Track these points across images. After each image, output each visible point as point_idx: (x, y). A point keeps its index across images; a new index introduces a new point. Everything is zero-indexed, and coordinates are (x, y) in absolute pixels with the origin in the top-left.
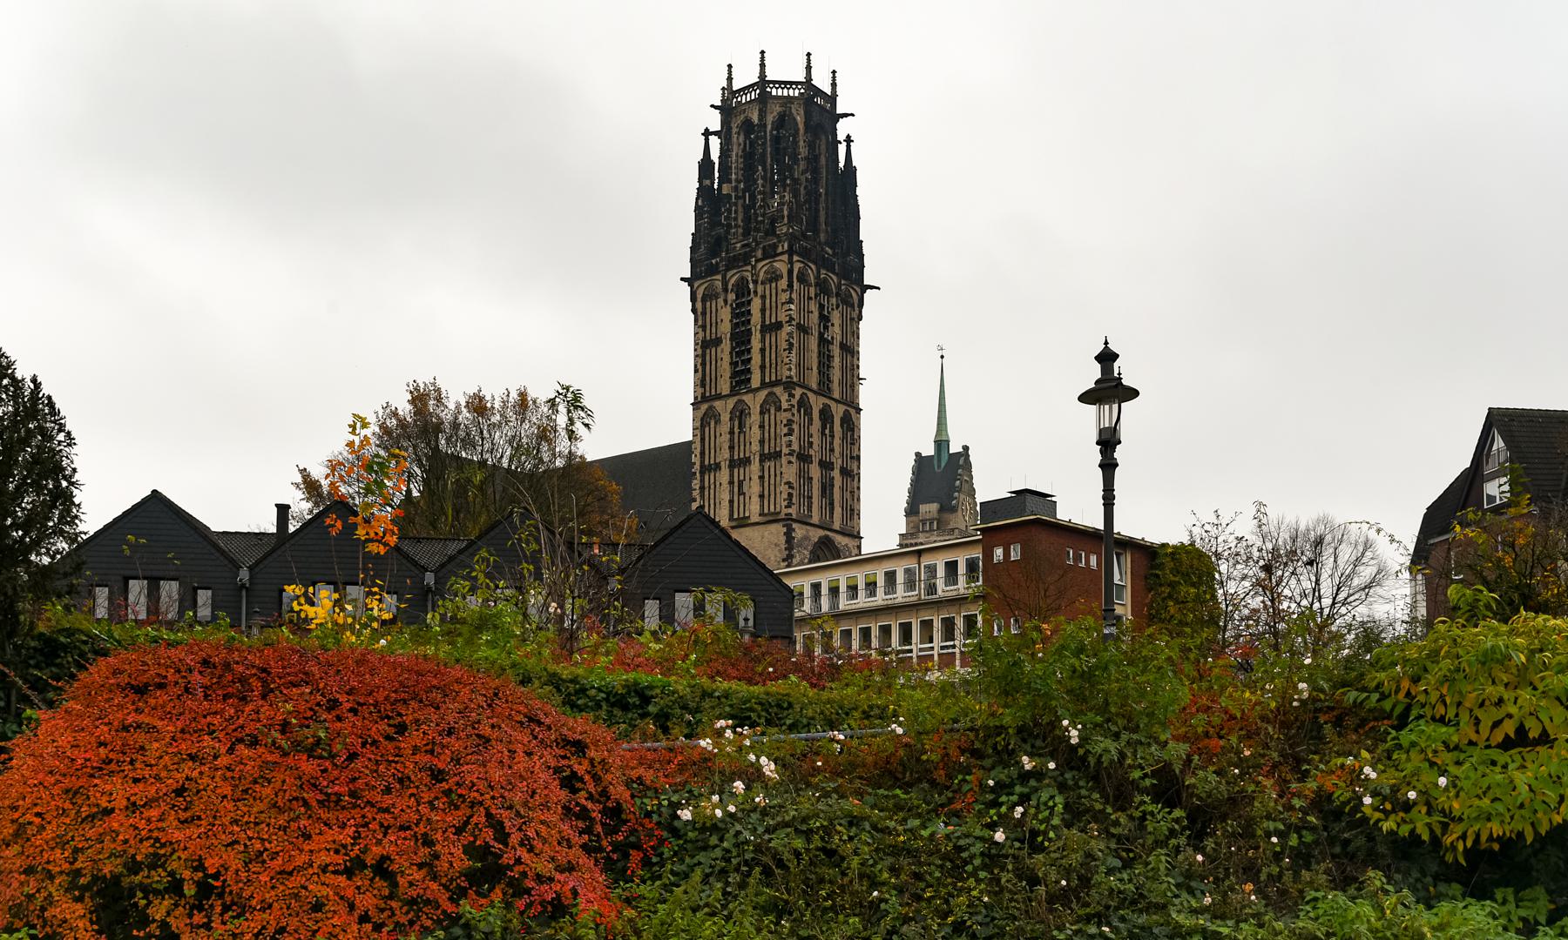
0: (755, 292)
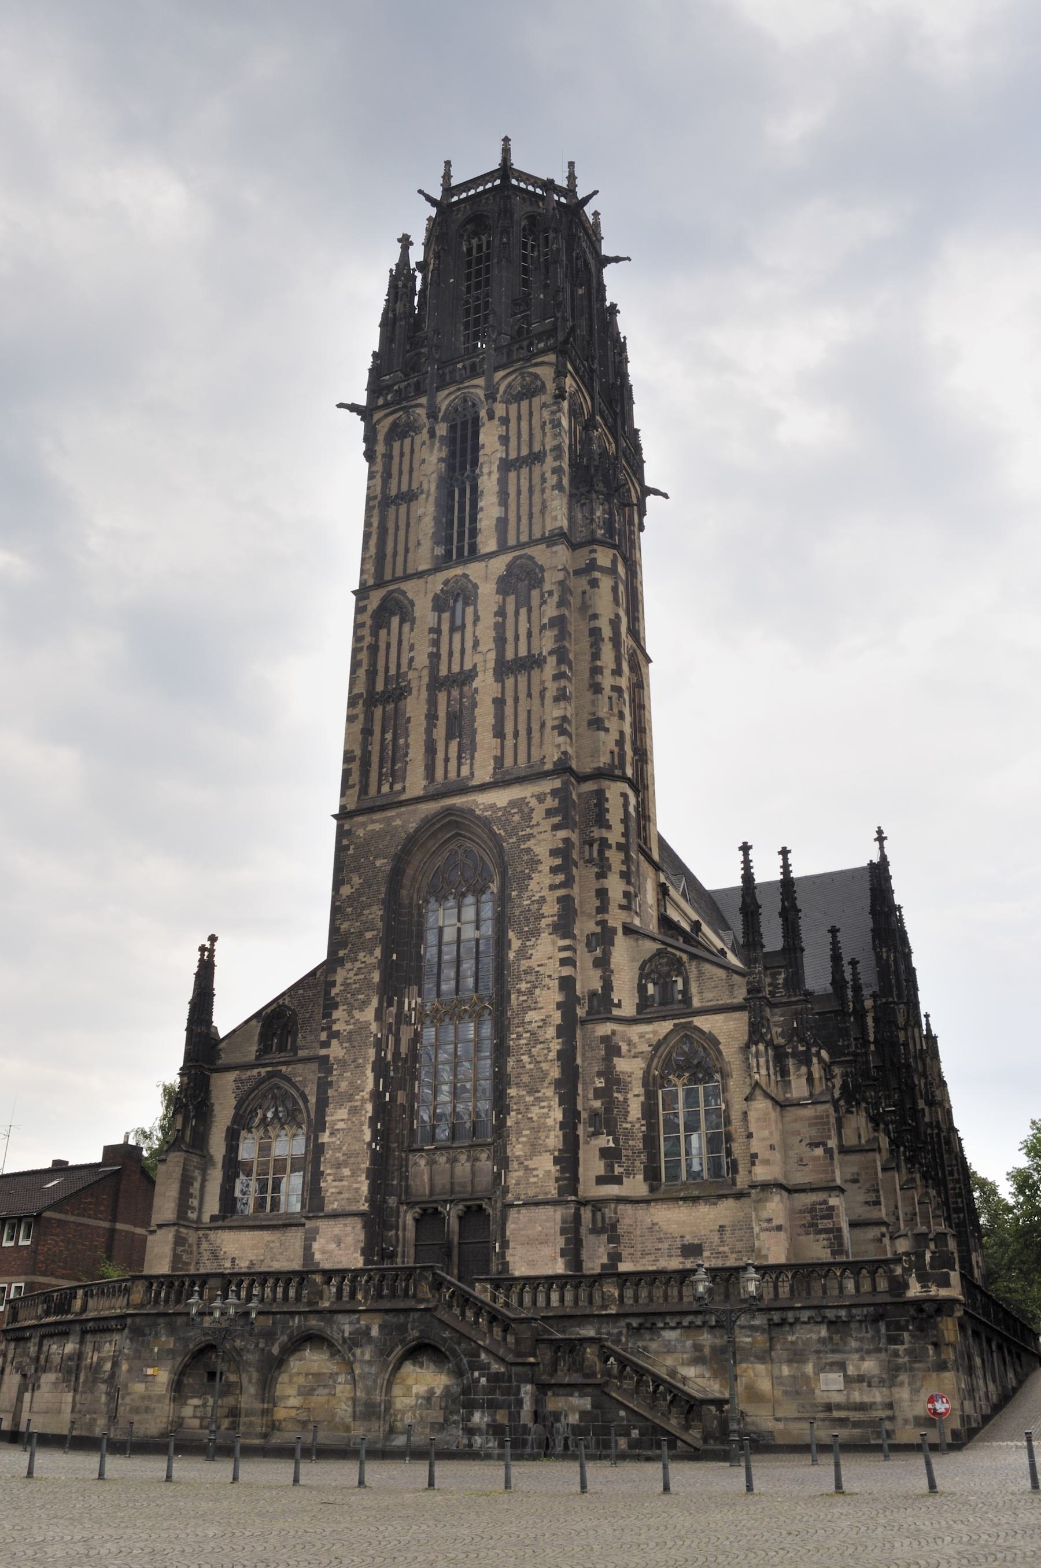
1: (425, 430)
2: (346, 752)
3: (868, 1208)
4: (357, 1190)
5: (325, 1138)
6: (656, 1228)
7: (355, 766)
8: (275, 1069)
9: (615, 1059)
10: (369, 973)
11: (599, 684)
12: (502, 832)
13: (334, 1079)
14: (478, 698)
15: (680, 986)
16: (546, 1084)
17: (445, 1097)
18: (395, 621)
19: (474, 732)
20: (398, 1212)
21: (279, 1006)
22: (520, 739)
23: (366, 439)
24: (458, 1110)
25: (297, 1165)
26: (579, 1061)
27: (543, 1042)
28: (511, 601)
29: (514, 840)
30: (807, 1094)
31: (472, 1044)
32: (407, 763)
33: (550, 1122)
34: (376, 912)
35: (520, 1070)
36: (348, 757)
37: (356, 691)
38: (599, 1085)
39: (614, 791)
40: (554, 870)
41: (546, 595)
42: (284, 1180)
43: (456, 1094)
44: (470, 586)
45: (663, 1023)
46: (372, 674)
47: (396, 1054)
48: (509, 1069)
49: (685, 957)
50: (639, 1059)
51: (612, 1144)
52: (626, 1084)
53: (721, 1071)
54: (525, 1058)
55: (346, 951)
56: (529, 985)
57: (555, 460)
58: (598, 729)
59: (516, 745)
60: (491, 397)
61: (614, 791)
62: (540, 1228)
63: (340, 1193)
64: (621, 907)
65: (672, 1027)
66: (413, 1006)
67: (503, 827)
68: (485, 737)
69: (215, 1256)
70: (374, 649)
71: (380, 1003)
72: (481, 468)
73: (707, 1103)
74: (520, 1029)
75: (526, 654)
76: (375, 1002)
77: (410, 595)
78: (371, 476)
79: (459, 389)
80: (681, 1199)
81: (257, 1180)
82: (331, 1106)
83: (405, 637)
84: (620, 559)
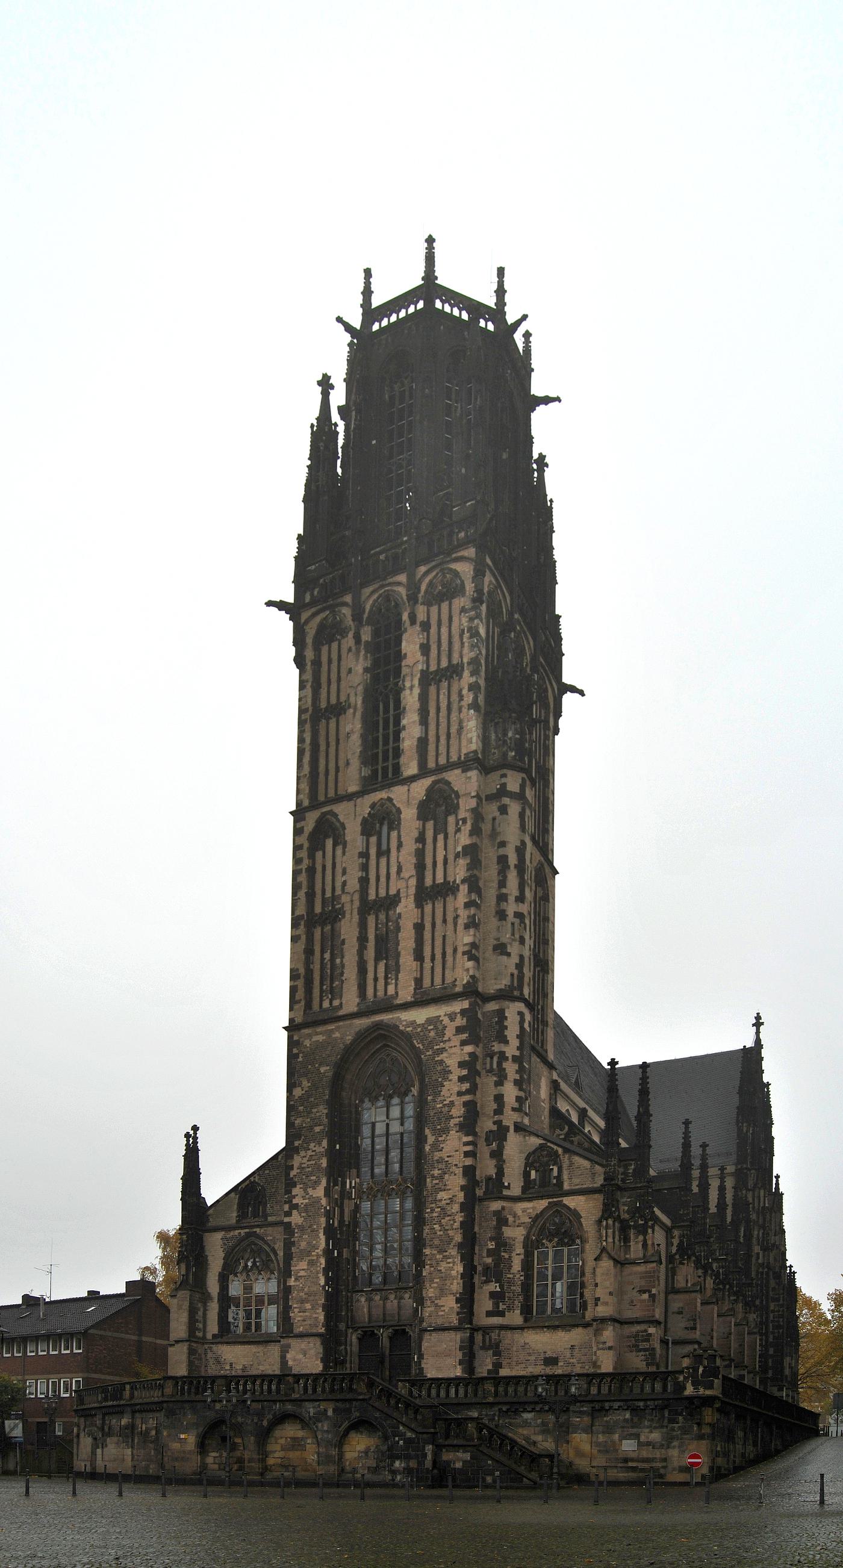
0: (413, 619)
1: (351, 635)
3: (686, 1332)
5: (292, 1282)
9: (503, 1227)
10: (319, 1159)
11: (504, 911)
13: (296, 1239)
14: (401, 922)
15: (555, 1173)
16: (451, 1246)
17: (378, 1253)
19: (398, 955)
20: (347, 1335)
22: (436, 962)
24: (388, 1262)
26: (476, 1229)
27: (450, 1216)
29: (430, 1053)
30: (641, 1255)
31: (398, 1214)
33: (454, 1273)
38: (491, 1247)
39: (513, 1010)
40: (461, 1079)
43: (386, 1251)
44: (394, 810)
45: (540, 1201)
47: (341, 1221)
48: (425, 1235)
49: (560, 1151)
50: (522, 1228)
51: (498, 1289)
52: (511, 1246)
53: (581, 1238)
56: (440, 1172)
57: (472, 675)
58: (501, 954)
59: (433, 968)
60: (413, 598)
61: (513, 1010)
64: (514, 1109)
66: (353, 1185)
67: (422, 1042)
72: (404, 681)
73: (569, 1261)
74: (433, 1205)
75: (442, 881)
76: (324, 1182)
79: (382, 586)
80: (545, 1327)
83: (338, 860)
84: (528, 782)
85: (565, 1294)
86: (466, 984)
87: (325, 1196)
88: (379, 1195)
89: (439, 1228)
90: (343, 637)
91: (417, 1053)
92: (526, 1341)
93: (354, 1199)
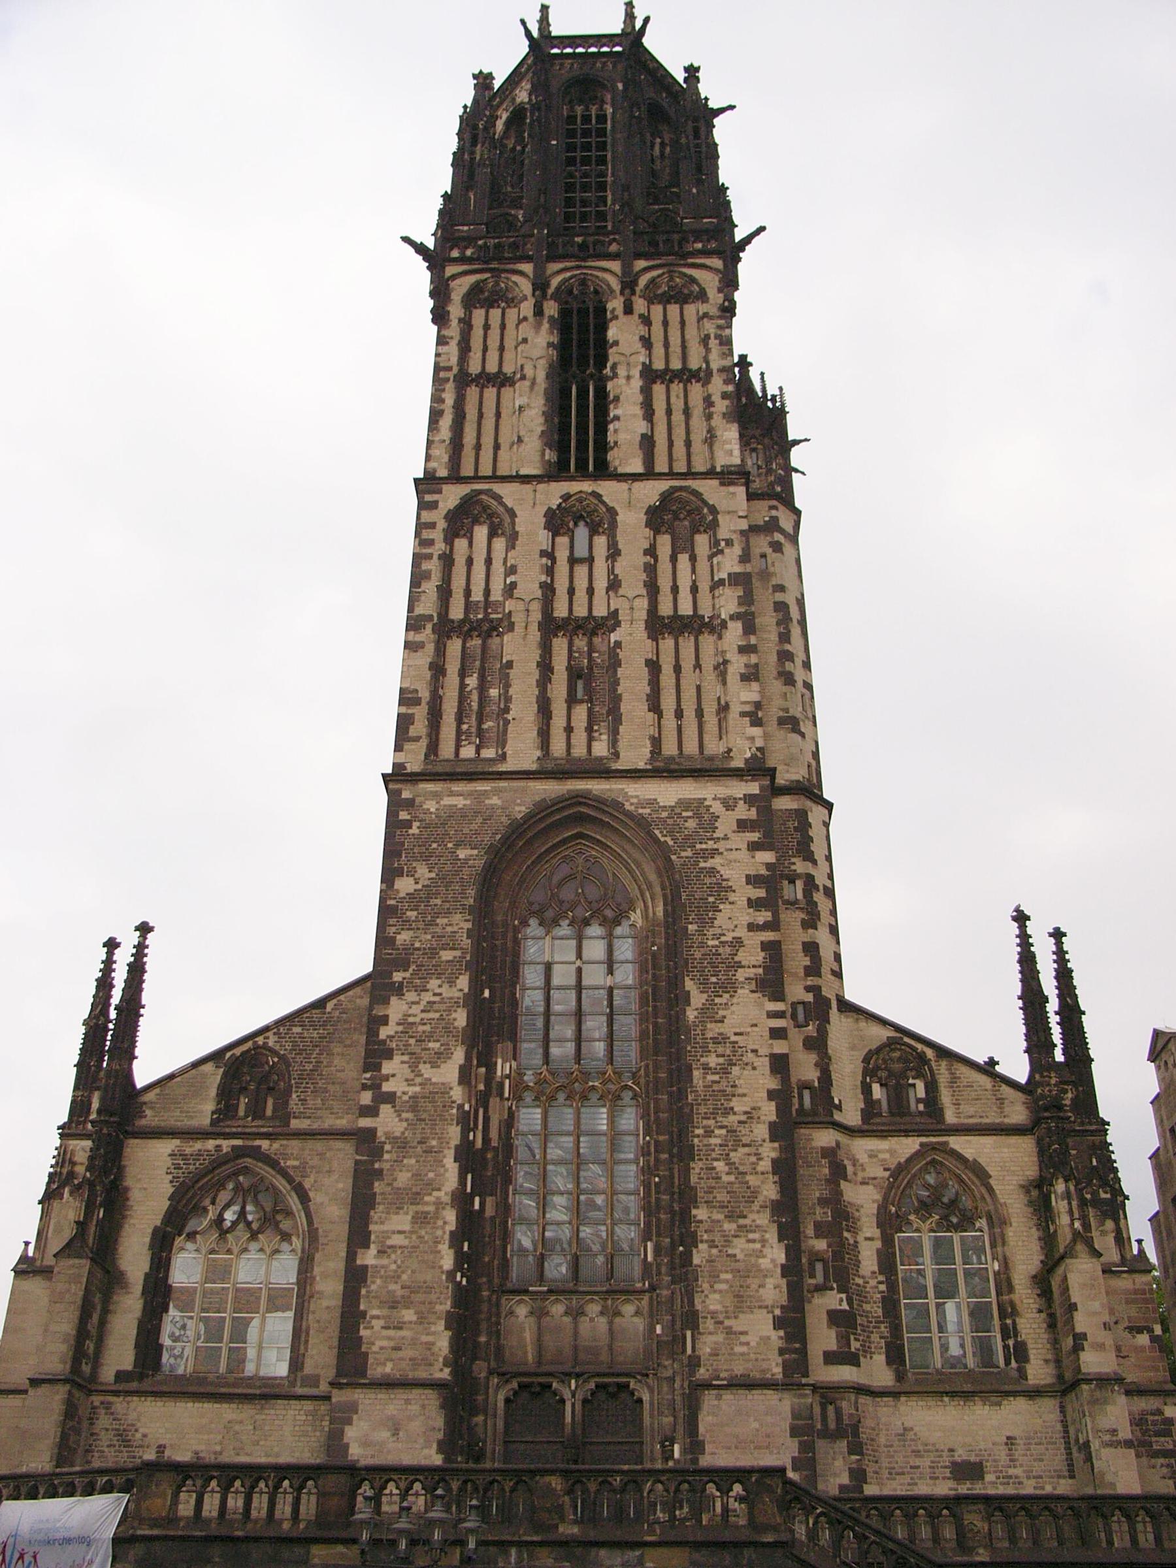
2: (402, 691)
4: (429, 1346)
5: (368, 1257)
6: (910, 1435)
7: (420, 713)
8: (250, 1143)
12: (668, 839)
16: (756, 1206)
18: (481, 533)
21: (256, 1047)
22: (685, 721)
23: (433, 294)
24: (582, 1235)
25: (276, 1301)
28: (664, 544)
29: (689, 853)
32: (507, 722)
33: (765, 1263)
34: (460, 924)
35: (712, 1182)
36: (406, 698)
37: (419, 610)
40: (753, 904)
41: (723, 544)
42: (255, 1323)
43: (578, 1212)
46: (445, 593)
48: (694, 1179)
49: (930, 1053)
50: (871, 1187)
51: (845, 1306)
54: (720, 1166)
55: (407, 975)
59: (680, 729)
62: (756, 1425)
63: (399, 1349)
65: (917, 1147)
67: (671, 833)
68: (634, 706)
69: (124, 1438)
70: (447, 560)
71: (468, 1058)
74: (711, 1122)
76: (459, 1056)
77: (509, 503)
78: (441, 341)
81: (205, 1320)
82: (381, 1208)
85: (967, 1327)
86: (751, 758)
87: (460, 1083)
88: (561, 1097)
89: (727, 1168)
90: (509, 307)
91: (664, 852)
92: (907, 1425)
93: (508, 1099)
